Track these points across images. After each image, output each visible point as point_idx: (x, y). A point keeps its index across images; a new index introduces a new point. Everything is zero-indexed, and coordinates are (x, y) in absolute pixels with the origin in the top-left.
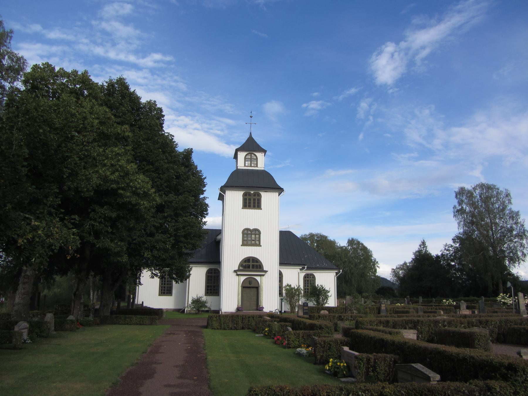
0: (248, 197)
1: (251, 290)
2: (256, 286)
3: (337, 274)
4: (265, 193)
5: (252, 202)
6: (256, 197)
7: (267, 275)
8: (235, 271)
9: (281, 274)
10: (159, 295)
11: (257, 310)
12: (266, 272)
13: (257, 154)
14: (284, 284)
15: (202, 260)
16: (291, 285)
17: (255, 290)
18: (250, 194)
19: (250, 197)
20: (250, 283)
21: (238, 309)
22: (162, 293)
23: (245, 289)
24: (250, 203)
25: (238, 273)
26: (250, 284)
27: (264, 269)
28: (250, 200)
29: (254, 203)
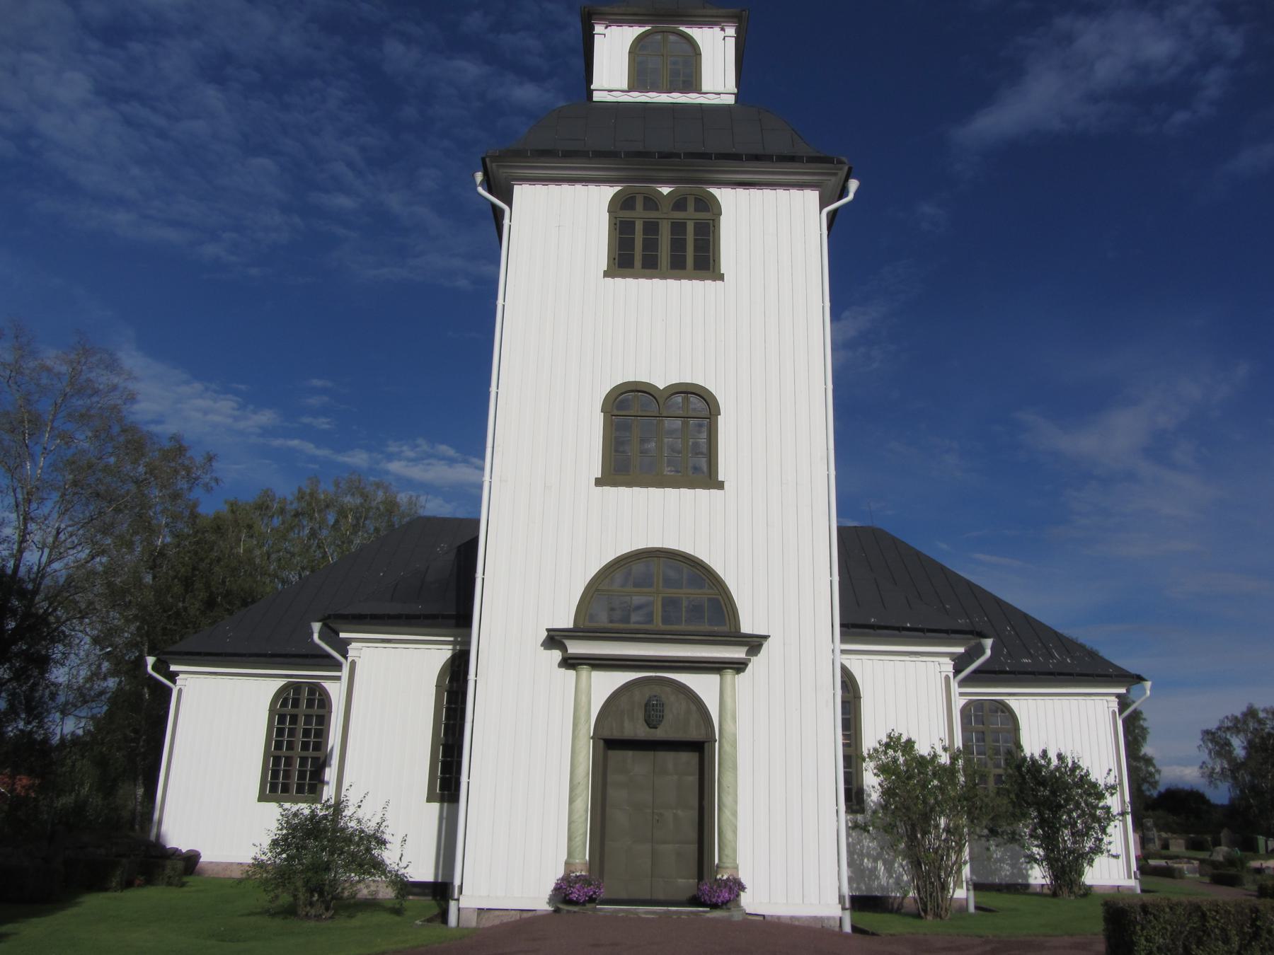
0: (639, 215)
1: (656, 761)
2: (694, 734)
3: (1123, 703)
4: (741, 192)
5: (665, 241)
6: (690, 215)
7: (757, 663)
8: (554, 639)
9: (850, 687)
10: (262, 798)
11: (695, 901)
12: (755, 644)
13: (695, 33)
14: (871, 738)
15: (419, 608)
16: (910, 744)
17: (689, 758)
18: (652, 202)
19: (652, 215)
20: (653, 714)
21: (564, 894)
22: (274, 788)
23: (616, 755)
24: (651, 244)
25: (576, 648)
26: (651, 723)
27: (746, 628)
28: (651, 227)
29: (678, 244)
